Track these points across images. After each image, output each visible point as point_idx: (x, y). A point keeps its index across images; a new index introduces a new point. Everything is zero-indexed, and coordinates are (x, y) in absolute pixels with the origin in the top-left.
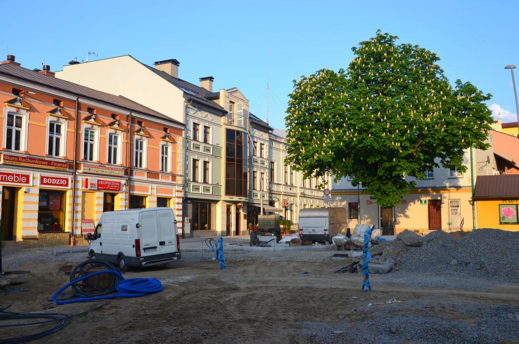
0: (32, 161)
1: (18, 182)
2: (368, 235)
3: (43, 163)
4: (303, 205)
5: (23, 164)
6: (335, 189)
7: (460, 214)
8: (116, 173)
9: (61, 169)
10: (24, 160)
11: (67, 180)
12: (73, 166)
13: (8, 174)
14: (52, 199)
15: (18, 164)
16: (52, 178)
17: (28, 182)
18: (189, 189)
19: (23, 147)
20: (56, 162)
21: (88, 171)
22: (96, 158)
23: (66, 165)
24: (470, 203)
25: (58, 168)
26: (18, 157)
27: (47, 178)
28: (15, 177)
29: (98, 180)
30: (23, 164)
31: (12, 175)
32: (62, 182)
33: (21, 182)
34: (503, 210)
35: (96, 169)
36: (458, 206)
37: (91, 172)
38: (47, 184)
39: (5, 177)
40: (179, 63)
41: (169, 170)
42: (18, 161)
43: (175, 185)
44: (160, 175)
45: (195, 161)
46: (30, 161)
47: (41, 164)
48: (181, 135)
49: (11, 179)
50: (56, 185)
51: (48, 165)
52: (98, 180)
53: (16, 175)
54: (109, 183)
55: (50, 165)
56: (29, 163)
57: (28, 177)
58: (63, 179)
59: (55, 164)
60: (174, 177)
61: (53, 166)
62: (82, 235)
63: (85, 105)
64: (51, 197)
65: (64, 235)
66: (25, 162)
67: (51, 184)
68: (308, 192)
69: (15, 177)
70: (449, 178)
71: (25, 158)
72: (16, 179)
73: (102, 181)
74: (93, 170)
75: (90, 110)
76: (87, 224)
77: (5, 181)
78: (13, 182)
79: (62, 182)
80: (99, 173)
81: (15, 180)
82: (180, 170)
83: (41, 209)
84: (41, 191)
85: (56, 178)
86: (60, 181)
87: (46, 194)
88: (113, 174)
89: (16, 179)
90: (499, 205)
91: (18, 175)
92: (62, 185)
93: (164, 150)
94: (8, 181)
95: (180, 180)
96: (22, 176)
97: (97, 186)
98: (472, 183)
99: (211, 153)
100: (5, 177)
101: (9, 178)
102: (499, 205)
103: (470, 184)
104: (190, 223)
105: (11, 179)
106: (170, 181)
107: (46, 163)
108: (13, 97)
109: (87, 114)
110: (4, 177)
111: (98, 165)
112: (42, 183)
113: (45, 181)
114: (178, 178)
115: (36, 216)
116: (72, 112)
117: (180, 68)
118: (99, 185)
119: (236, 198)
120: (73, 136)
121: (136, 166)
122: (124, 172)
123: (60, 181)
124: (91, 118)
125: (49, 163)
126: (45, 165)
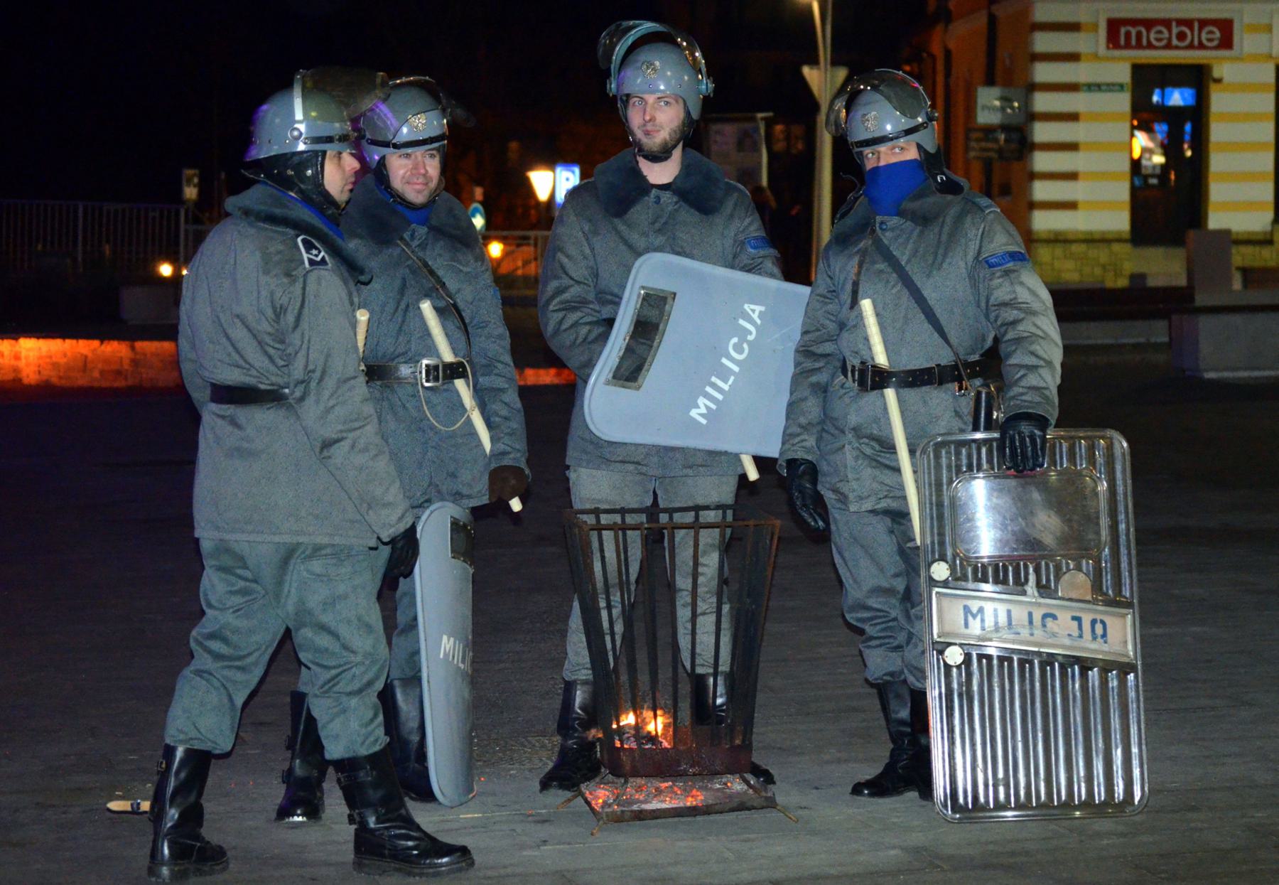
13: (1149, 24)
17: (1226, 42)
28: (1175, 30)
31: (1167, 23)
33: (1201, 46)
39: (1139, 35)
49: (1210, 40)
53: (1180, 22)
69: (1175, 30)
72: (1181, 36)
77: (1139, 46)
78: (1169, 46)
81: (1175, 42)
89: (1181, 36)
91: (1188, 23)
94: (1150, 46)
96: (1203, 23)
100: (1139, 35)
101: (1152, 36)
105: (1210, 40)
110: (1133, 31)
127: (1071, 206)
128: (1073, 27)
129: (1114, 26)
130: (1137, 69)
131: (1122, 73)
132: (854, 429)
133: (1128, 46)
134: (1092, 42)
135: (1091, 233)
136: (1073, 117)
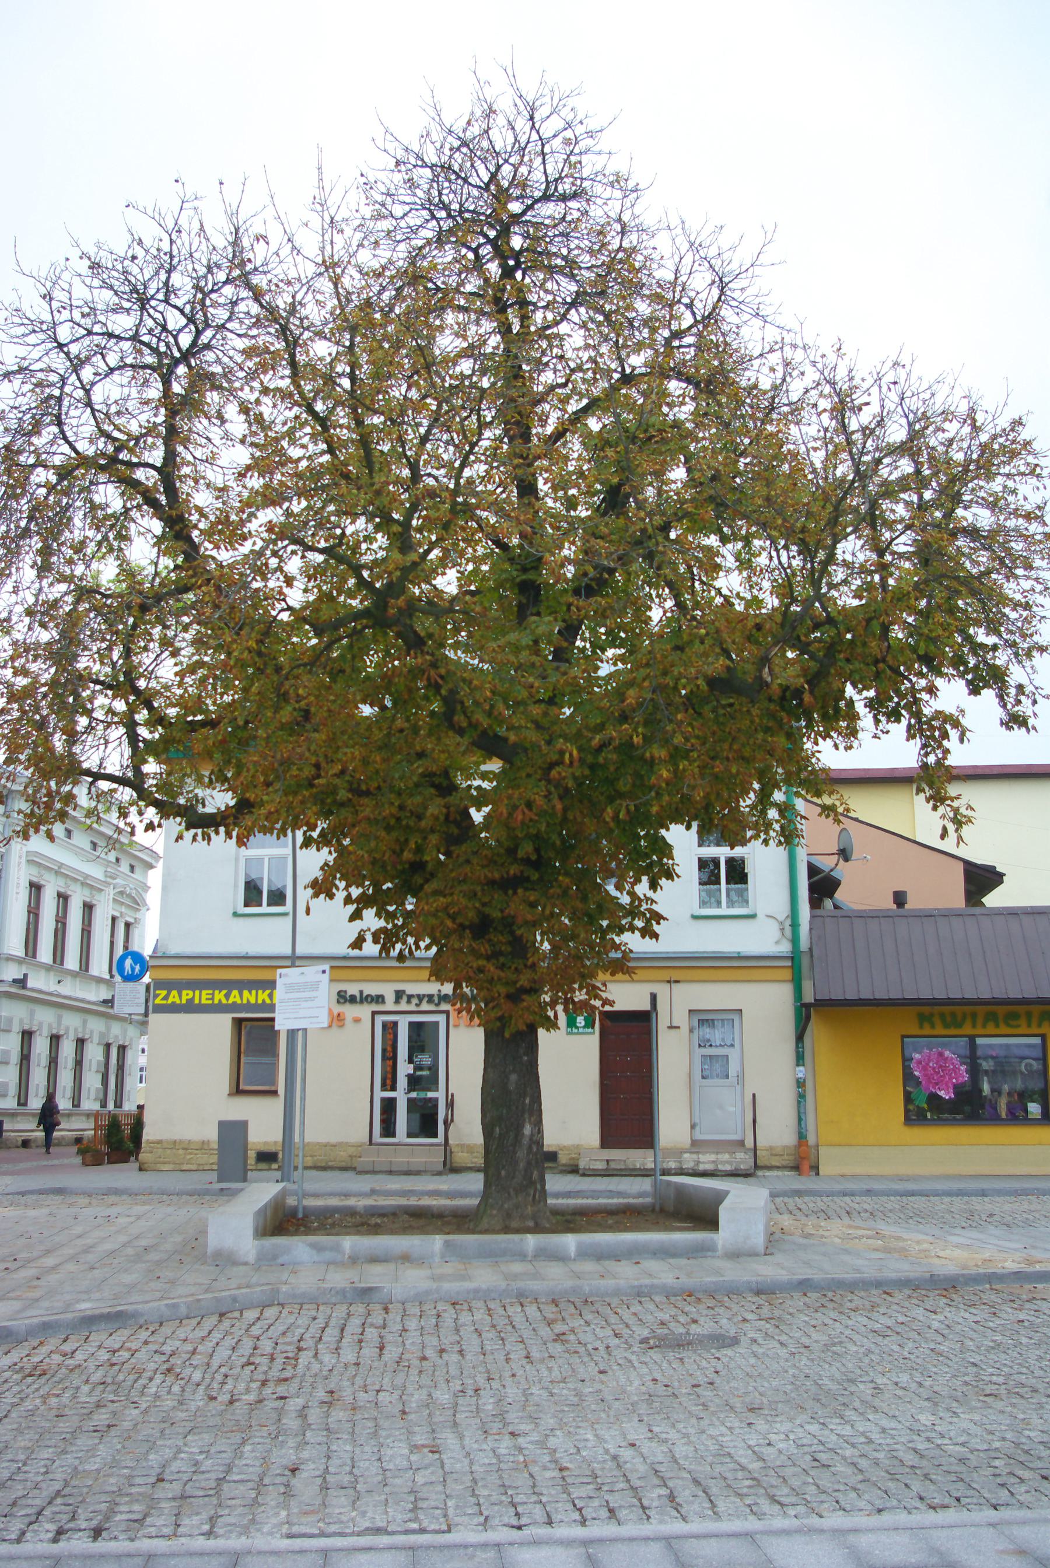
4: (16, 1028)
6: (173, 950)
7: (740, 1078)
34: (919, 1062)
36: (732, 1045)
68: (38, 981)
70: (695, 917)
90: (903, 1037)
98: (795, 940)
102: (903, 1037)
103: (785, 948)
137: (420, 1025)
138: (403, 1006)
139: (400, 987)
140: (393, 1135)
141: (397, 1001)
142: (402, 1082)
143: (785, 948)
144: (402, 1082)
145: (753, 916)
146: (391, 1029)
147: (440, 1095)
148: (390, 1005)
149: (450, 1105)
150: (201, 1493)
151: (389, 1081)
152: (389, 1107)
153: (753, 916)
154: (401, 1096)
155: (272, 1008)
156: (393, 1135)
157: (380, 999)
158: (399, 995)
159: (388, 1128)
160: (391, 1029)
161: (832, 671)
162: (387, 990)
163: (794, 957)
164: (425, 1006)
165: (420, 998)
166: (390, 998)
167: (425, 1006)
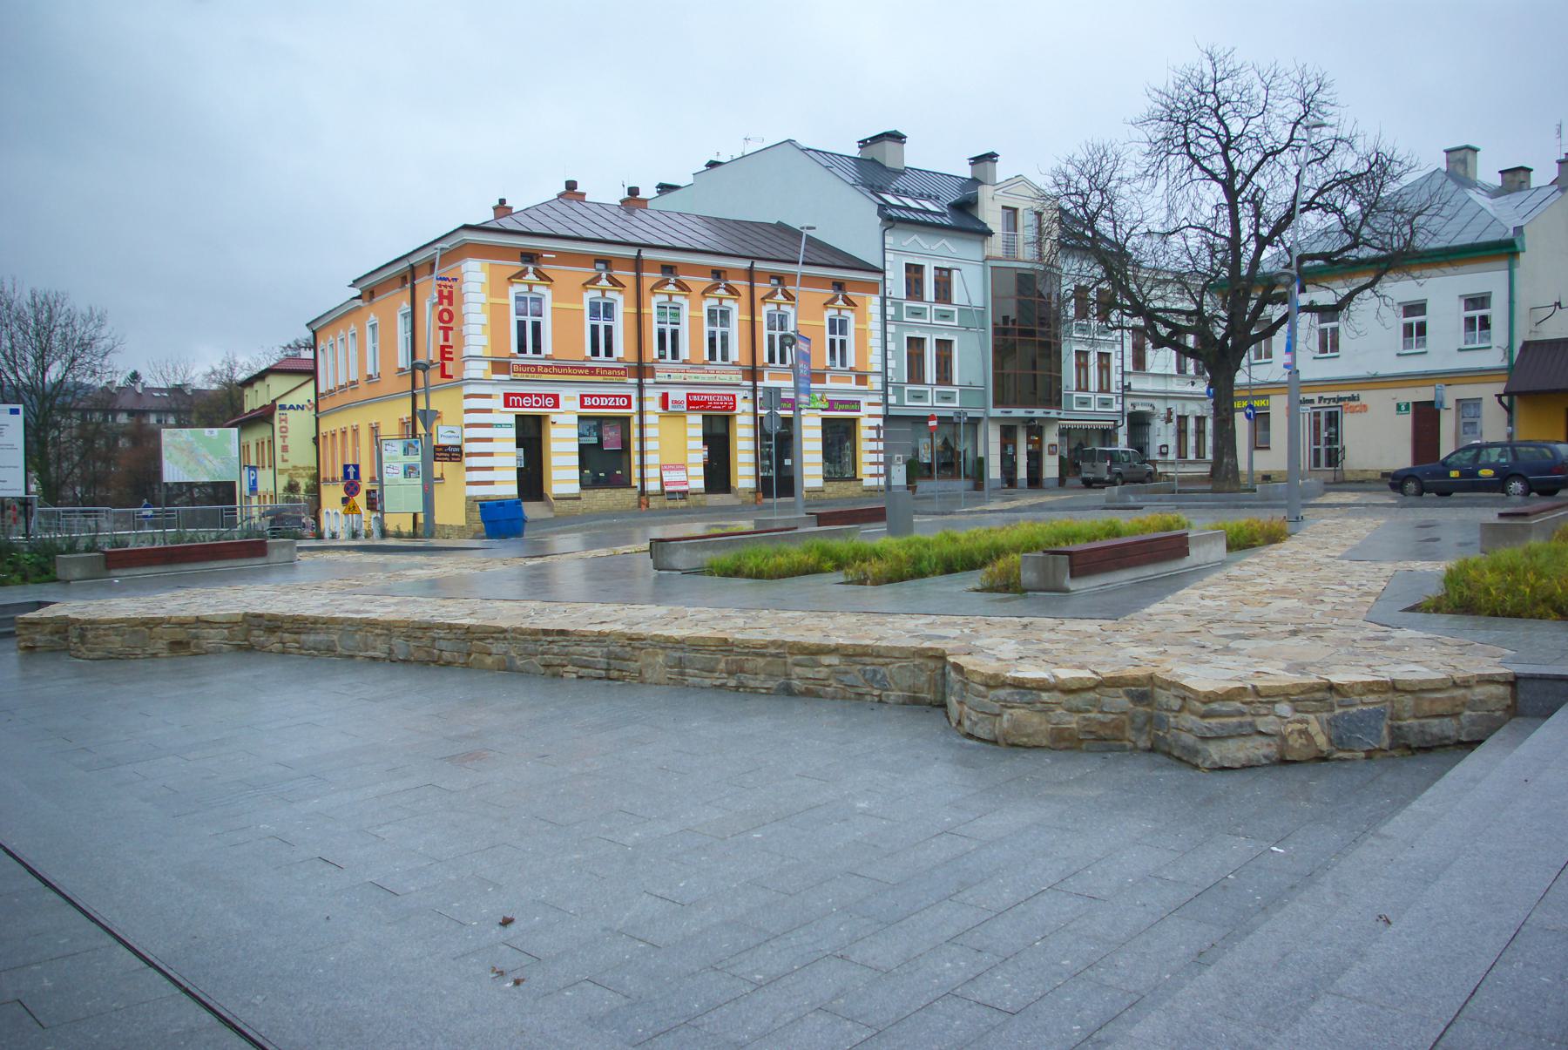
0: (564, 370)
1: (541, 407)
2: (1411, 486)
3: (581, 371)
5: (544, 377)
8: (725, 379)
9: (615, 379)
10: (546, 370)
11: (629, 397)
12: (641, 370)
13: (523, 396)
14: (607, 432)
15: (536, 377)
16: (599, 396)
17: (557, 405)
18: (900, 398)
19: (547, 347)
20: (604, 369)
21: (667, 380)
22: (685, 352)
23: (623, 372)
24: (1501, 402)
25: (608, 379)
26: (536, 366)
27: (591, 396)
29: (688, 395)
30: (544, 377)
31: (530, 395)
32: (619, 402)
33: (546, 407)
35: (683, 375)
37: (671, 380)
38: (592, 407)
40: (905, 137)
41: (851, 361)
42: (536, 372)
43: (866, 393)
44: (828, 377)
45: (916, 344)
46: (558, 370)
47: (578, 374)
48: (876, 292)
50: (608, 407)
51: (590, 374)
52: (688, 395)
53: (536, 395)
54: (711, 398)
55: (594, 374)
56: (555, 373)
57: (556, 397)
58: (620, 396)
59: (603, 372)
60: (862, 378)
61: (599, 375)
62: (662, 489)
63: (652, 261)
64: (605, 428)
65: (630, 491)
66: (548, 373)
67: (600, 407)
71: (548, 367)
72: (537, 402)
73: (696, 394)
74: (676, 377)
75: (668, 269)
76: (673, 473)
78: (531, 407)
79: (619, 402)
80: (688, 380)
82: (874, 362)
83: (583, 449)
84: (581, 418)
85: (607, 396)
86: (615, 401)
87: (595, 423)
88: (717, 381)
89: (537, 402)
91: (540, 396)
92: (620, 407)
93: (838, 326)
94: (523, 406)
95: (875, 383)
96: (547, 396)
97: (685, 405)
98: (1510, 359)
99: (956, 323)
101: (524, 401)
104: (905, 466)
106: (852, 385)
107: (587, 371)
108: (518, 265)
109: (658, 276)
111: (254, 400)
112: (582, 406)
113: (587, 401)
114: (871, 379)
115: (575, 460)
116: (626, 276)
117: (908, 147)
118: (690, 403)
119: (1019, 412)
120: (633, 320)
121: (772, 359)
122: (740, 376)
123: (615, 401)
124: (668, 284)
125: (592, 371)
126: (584, 374)
127: (491, 483)
128: (489, 396)
129: (507, 396)
130: (518, 417)
131: (513, 420)
132: (1475, 565)
133: (513, 406)
134: (498, 403)
135: (489, 496)
136: (490, 440)
137: (1330, 413)
138: (1322, 404)
139: (1321, 395)
140: (1319, 466)
141: (1320, 402)
142: (1323, 441)
143: (1505, 364)
144: (1323, 441)
145: (1490, 348)
146: (1317, 415)
147: (1339, 446)
148: (1316, 405)
149: (1343, 449)
150: (1245, 625)
151: (1317, 442)
152: (1317, 452)
153: (1490, 348)
154: (1323, 448)
155: (1268, 408)
156: (1319, 466)
157: (1312, 401)
158: (1320, 399)
159: (1317, 463)
160: (1317, 415)
161: (1222, 313)
162: (1315, 397)
163: (1511, 369)
164: (1332, 404)
165: (1330, 399)
166: (1316, 400)
167: (1332, 404)
